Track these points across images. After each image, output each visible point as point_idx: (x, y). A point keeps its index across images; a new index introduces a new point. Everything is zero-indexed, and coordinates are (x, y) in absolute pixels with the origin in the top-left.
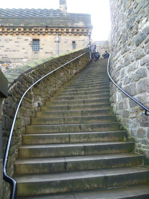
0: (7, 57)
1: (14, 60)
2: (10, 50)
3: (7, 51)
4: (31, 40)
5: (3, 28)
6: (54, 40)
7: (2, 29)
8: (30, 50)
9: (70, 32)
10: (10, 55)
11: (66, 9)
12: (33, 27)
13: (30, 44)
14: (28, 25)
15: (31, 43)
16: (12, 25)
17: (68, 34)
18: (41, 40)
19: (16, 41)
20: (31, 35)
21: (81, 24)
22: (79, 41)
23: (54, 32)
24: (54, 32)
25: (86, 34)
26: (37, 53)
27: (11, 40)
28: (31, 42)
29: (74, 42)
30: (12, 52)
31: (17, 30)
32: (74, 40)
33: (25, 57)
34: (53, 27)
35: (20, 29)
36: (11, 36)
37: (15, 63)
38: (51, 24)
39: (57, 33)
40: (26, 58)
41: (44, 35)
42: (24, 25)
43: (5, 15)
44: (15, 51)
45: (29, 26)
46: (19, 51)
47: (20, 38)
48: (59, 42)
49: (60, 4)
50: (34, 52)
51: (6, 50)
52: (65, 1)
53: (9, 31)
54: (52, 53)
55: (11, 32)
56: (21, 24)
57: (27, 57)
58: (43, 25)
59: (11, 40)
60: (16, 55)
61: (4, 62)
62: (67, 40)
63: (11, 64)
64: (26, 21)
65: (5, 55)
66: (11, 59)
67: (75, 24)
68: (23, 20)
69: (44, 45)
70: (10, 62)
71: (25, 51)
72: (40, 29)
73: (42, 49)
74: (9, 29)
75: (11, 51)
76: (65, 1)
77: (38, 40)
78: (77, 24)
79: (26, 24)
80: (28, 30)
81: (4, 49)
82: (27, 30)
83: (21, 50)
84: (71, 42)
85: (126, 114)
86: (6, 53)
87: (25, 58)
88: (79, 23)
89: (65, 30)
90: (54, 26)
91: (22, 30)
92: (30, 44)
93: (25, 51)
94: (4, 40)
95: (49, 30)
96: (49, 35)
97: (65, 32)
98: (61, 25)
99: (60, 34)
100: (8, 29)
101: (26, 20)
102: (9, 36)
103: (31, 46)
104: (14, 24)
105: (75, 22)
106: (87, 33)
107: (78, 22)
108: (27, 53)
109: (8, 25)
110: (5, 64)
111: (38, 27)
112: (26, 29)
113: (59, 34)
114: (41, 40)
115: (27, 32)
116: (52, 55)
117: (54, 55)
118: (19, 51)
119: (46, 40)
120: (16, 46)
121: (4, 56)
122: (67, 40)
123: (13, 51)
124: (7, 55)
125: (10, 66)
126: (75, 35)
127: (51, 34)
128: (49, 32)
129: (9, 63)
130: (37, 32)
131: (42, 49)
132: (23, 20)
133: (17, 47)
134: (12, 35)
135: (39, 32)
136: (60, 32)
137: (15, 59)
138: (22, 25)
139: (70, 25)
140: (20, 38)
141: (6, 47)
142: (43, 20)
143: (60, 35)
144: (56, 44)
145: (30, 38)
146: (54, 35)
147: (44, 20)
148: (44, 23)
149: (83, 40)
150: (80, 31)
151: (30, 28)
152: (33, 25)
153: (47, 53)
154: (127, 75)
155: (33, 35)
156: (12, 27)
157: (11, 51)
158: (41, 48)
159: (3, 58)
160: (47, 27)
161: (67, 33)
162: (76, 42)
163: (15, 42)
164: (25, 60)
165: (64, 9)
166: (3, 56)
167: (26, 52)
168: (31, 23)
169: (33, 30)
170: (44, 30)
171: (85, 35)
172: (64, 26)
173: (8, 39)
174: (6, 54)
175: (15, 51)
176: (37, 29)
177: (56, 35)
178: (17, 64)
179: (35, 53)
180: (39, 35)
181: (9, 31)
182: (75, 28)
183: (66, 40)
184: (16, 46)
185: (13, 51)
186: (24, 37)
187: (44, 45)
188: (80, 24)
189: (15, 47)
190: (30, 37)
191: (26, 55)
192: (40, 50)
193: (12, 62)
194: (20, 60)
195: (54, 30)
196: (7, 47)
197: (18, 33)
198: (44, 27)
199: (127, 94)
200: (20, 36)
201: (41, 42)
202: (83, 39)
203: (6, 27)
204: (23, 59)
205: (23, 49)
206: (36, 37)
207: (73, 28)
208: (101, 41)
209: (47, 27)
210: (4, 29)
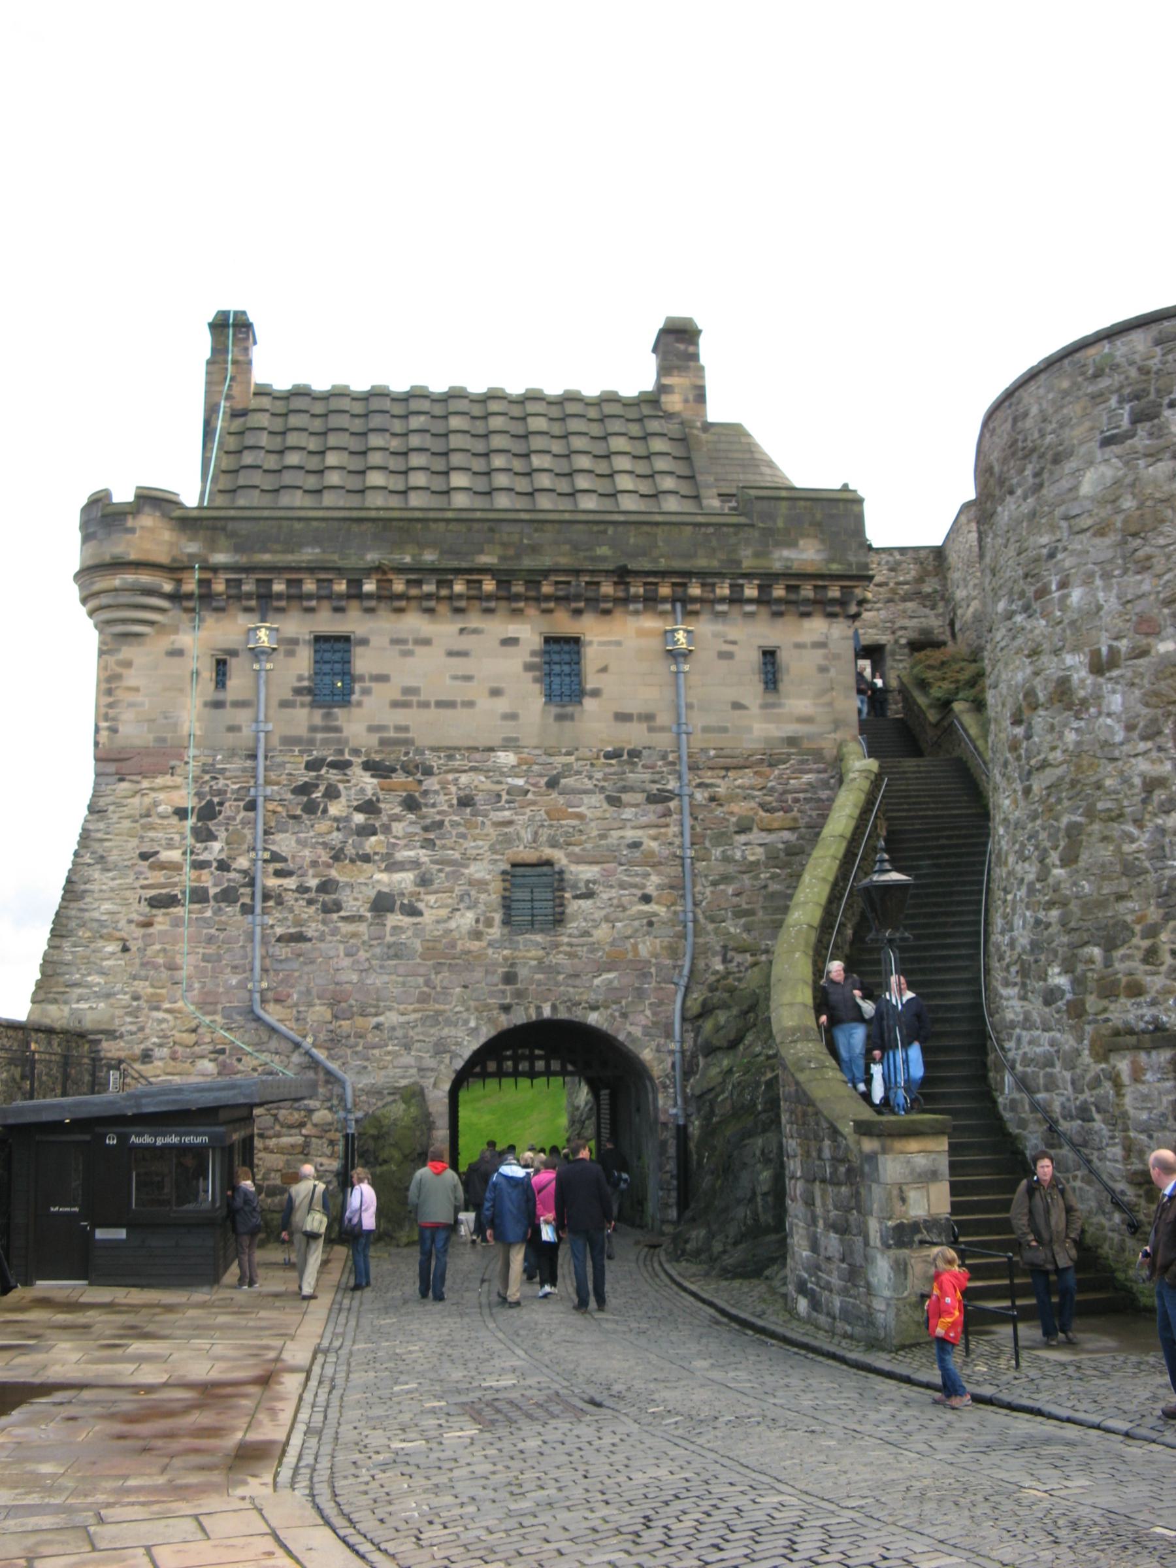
0: (408, 742)
1: (450, 757)
2: (422, 698)
3: (405, 705)
4: (536, 642)
5: (384, 573)
6: (655, 644)
7: (378, 581)
8: (532, 701)
9: (750, 601)
10: (426, 728)
11: (700, 396)
12: (546, 573)
13: (528, 667)
14: (518, 557)
15: (537, 660)
16: (430, 557)
17: (736, 609)
18: (591, 643)
19: (456, 648)
20: (532, 611)
21: (807, 554)
22: (799, 646)
23: (664, 600)
24: (664, 600)
25: (837, 609)
26: (571, 717)
27: (426, 642)
28: (533, 653)
29: (769, 655)
30: (433, 713)
31: (459, 587)
32: (770, 642)
33: (507, 739)
34: (654, 573)
35: (480, 582)
36: (426, 616)
37: (450, 777)
38: (644, 554)
39: (678, 606)
40: (510, 744)
41: (607, 612)
42: (502, 558)
43: (306, 417)
44: (451, 704)
45: (527, 563)
46: (470, 704)
47: (475, 631)
48: (686, 655)
49: (664, 370)
50: (554, 710)
51: (398, 696)
52: (691, 349)
53: (414, 592)
54: (648, 717)
55: (429, 596)
56: (481, 552)
57: (516, 739)
58: (604, 559)
59: (426, 642)
60: (457, 728)
61: (394, 770)
62: (734, 643)
63: (432, 783)
64: (505, 538)
65: (398, 729)
66: (433, 749)
67: (776, 554)
68: (491, 530)
69: (604, 670)
70: (428, 772)
71: (502, 705)
72: (587, 583)
73: (596, 693)
74: (419, 583)
75: (425, 705)
76: (691, 349)
77: (576, 641)
78: (786, 553)
79: (511, 552)
80: (518, 588)
81: (391, 691)
82: (515, 588)
83: (485, 703)
84: (755, 657)
85: (1023, 1124)
86: (401, 717)
87: (505, 748)
88: (801, 543)
89: (724, 590)
90: (663, 564)
91: (489, 586)
92: (528, 667)
93: (502, 705)
94: (385, 641)
95: (637, 589)
96: (636, 613)
97: (722, 600)
98: (702, 562)
99: (686, 606)
100: (408, 582)
101: (506, 528)
102: (414, 623)
103: (536, 680)
104: (442, 553)
105: (779, 544)
106: (843, 603)
107: (793, 544)
108: (513, 716)
109: (408, 559)
110: (399, 778)
111: (577, 572)
112: (509, 582)
113: (690, 607)
114: (591, 643)
115: (517, 597)
116: (651, 730)
117: (662, 729)
118: (470, 704)
119: (618, 643)
120: (455, 678)
121: (392, 734)
122: (734, 643)
123: (440, 704)
124: (406, 729)
125: (425, 793)
126: (778, 615)
127: (646, 609)
128: (635, 599)
129: (419, 776)
130: (566, 599)
131: (596, 693)
132: (491, 530)
133: (458, 683)
134: (430, 611)
135: (577, 598)
136: (694, 600)
137: (450, 752)
138: (486, 559)
139: (748, 563)
140: (475, 631)
141: (401, 680)
142: (602, 527)
143: (696, 613)
144: (673, 668)
145: (528, 632)
146: (663, 613)
147: (605, 532)
148: (603, 551)
149: (821, 645)
150: (807, 592)
151: (534, 578)
152: (547, 562)
153: (622, 717)
154: (1027, 1049)
155: (548, 616)
156: (434, 571)
157: (425, 705)
158: (589, 686)
159: (383, 742)
160: (622, 575)
161: (736, 599)
162: (784, 656)
163: (451, 654)
164: (507, 758)
165: (686, 401)
166: (385, 735)
167: (508, 710)
168: (535, 549)
169: (547, 589)
170: (607, 589)
171: (831, 615)
172: (715, 564)
173: (410, 638)
174: (403, 723)
175: (451, 704)
176: (568, 583)
177: (674, 610)
178: (464, 779)
179: (560, 718)
180: (578, 612)
181: (414, 592)
182: (775, 577)
183: (726, 642)
184: (455, 678)
185: (440, 704)
186: (499, 626)
187: (604, 670)
188: (804, 556)
189: (448, 681)
190: (528, 627)
191: (508, 730)
192: (589, 703)
193: (435, 770)
194: (477, 756)
195: (665, 591)
196: (412, 683)
197: (462, 604)
198: (607, 572)
199: (1023, 1084)
200: (474, 620)
201: (592, 656)
202: (822, 639)
203: (401, 570)
204: (491, 749)
205: (496, 692)
206: (563, 623)
207: (767, 579)
208: (903, 550)
209: (622, 575)
210: (390, 581)
